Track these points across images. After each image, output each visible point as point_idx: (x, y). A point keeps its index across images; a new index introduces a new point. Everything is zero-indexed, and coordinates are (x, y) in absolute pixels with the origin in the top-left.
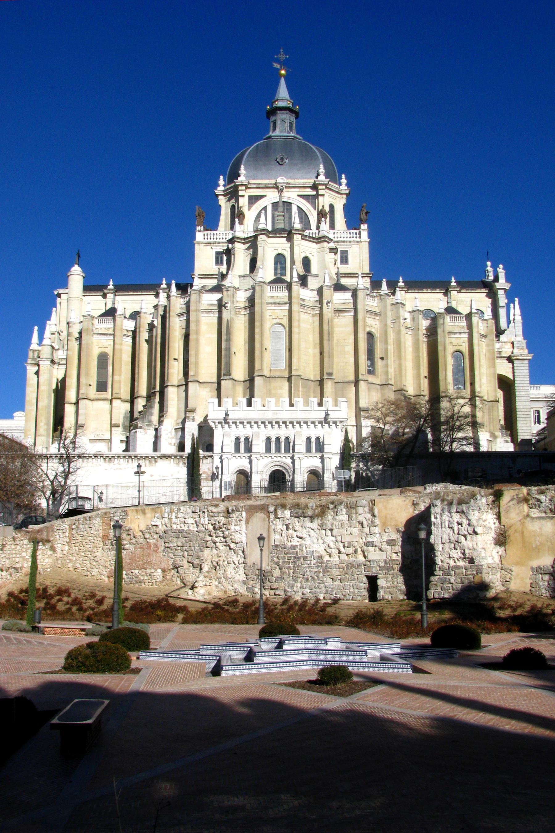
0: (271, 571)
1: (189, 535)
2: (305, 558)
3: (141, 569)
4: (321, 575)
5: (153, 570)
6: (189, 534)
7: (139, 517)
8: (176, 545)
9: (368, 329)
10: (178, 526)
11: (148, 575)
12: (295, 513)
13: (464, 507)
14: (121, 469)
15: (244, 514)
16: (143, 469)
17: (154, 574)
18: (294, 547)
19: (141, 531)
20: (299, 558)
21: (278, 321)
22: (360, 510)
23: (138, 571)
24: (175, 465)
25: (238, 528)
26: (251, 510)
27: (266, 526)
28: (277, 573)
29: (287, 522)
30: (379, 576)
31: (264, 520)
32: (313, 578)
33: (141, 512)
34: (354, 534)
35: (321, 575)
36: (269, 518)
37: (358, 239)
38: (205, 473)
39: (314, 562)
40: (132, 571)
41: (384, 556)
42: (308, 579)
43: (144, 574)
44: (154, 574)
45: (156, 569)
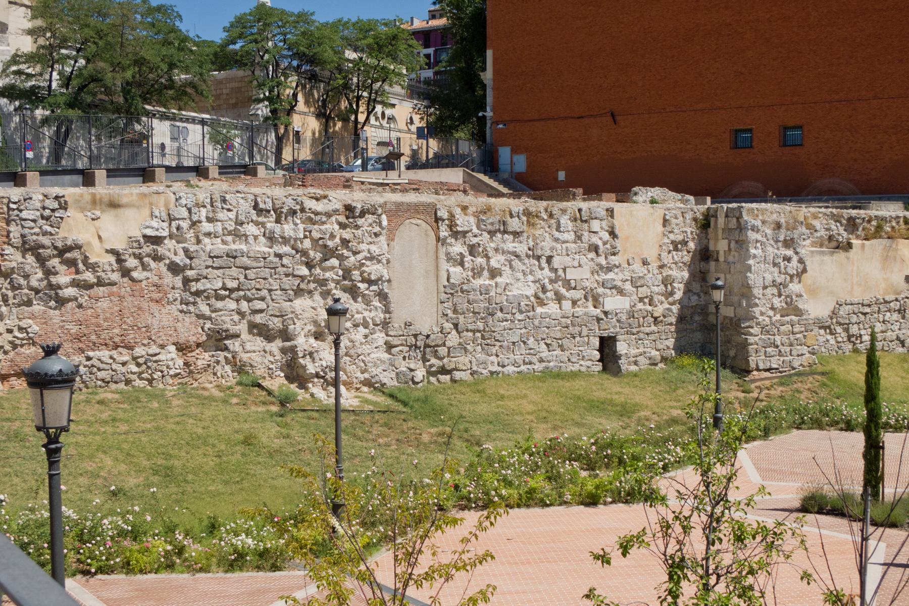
1: (255, 264)
3: (116, 347)
5: (154, 349)
6: (256, 259)
7: (98, 213)
8: (220, 285)
11: (141, 361)
17: (160, 357)
19: (113, 252)
22: (595, 225)
23: (107, 353)
30: (619, 337)
31: (427, 235)
40: (91, 354)
43: (126, 358)
44: (160, 357)
45: (162, 347)
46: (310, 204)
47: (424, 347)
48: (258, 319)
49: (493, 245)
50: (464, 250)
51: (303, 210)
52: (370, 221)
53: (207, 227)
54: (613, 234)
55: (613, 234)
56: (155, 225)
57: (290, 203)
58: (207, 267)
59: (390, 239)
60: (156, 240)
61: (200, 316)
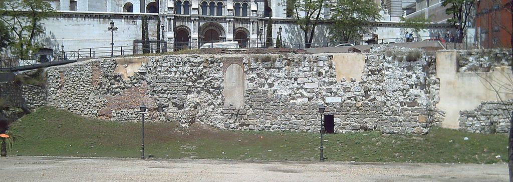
8: (161, 88)
13: (411, 63)
14: (78, 25)
16: (115, 26)
18: (265, 92)
22: (321, 64)
24: (125, 23)
25: (217, 76)
26: (229, 62)
29: (259, 72)
34: (314, 84)
38: (151, 30)
41: (339, 100)
46: (192, 59)
47: (238, 114)
48: (174, 101)
49: (268, 73)
50: (254, 75)
51: (190, 62)
52: (215, 65)
53: (159, 69)
54: (331, 67)
55: (331, 67)
56: (142, 68)
57: (185, 60)
58: (157, 82)
59: (224, 72)
60: (143, 74)
61: (155, 99)
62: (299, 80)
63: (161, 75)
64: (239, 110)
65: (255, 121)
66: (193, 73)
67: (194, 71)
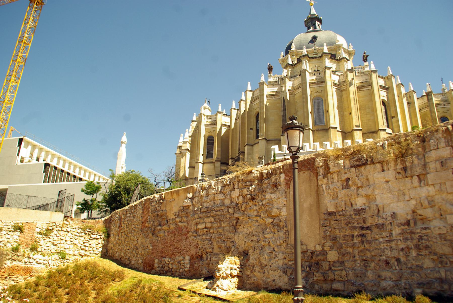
0: (324, 253)
2: (380, 227)
4: (414, 253)
9: (382, 98)
10: (208, 204)
12: (356, 161)
15: (283, 176)
20: (368, 228)
21: (318, 94)
27: (314, 188)
28: (333, 256)
32: (398, 260)
33: (175, 194)
35: (414, 253)
36: (317, 176)
37: (363, 71)
39: (396, 231)
42: (387, 263)
62: (430, 177)
63: (206, 205)
64: (313, 253)
65: (344, 273)
66: (244, 197)
67: (245, 192)
